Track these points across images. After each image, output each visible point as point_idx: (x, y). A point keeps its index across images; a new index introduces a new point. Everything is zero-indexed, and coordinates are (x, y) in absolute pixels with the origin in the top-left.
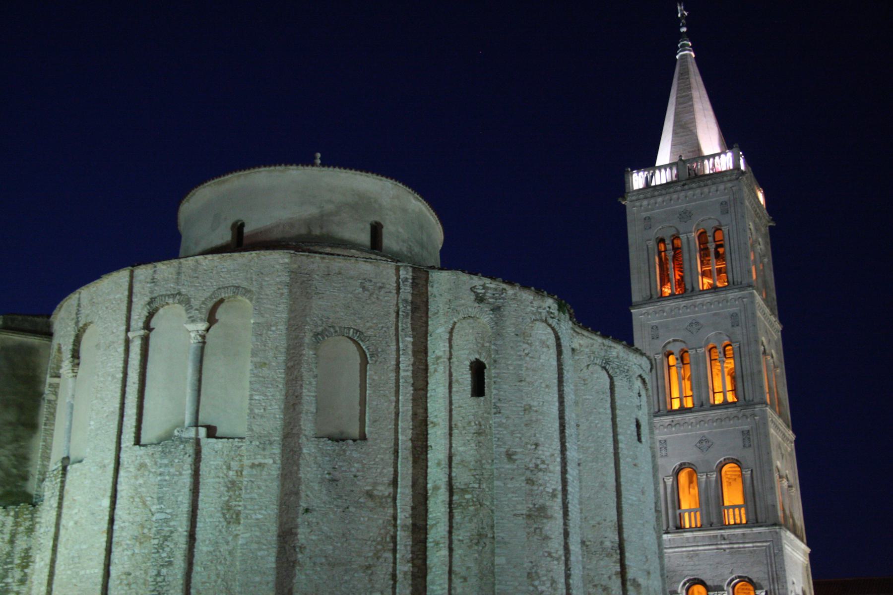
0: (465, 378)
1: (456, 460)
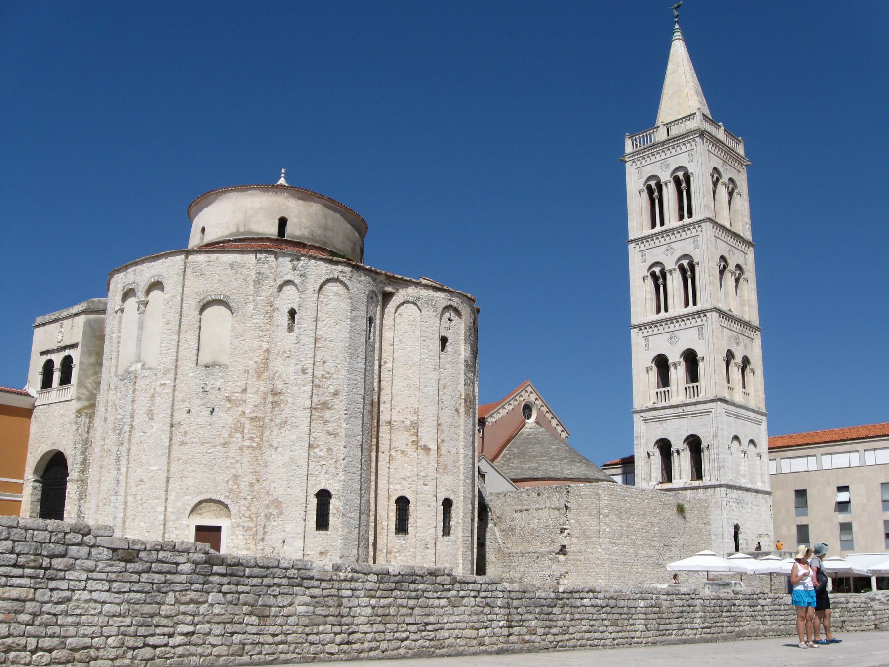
0: (285, 320)
1: (277, 375)
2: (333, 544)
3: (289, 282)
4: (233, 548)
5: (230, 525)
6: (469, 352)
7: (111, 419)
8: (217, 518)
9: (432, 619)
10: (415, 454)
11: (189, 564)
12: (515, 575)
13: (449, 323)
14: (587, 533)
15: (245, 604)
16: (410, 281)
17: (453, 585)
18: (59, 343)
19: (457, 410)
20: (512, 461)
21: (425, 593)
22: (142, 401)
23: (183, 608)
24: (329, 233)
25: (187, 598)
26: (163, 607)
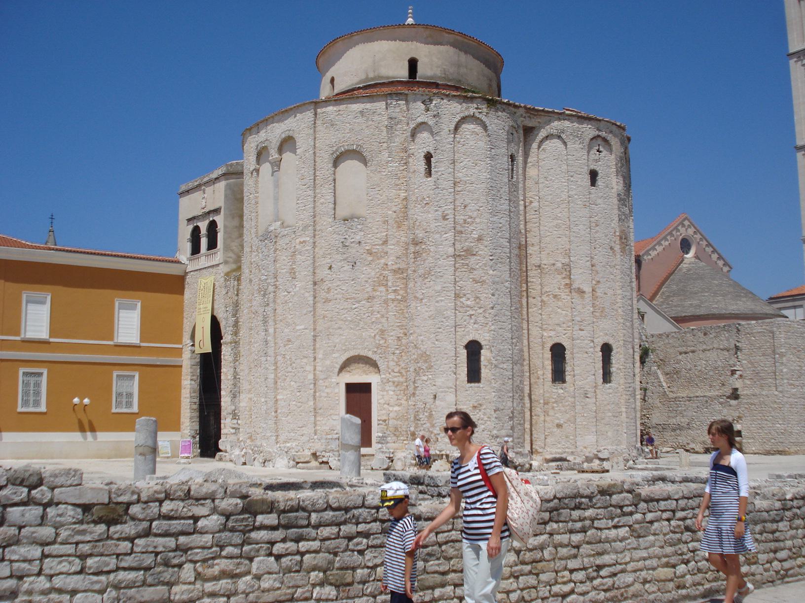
0: (421, 166)
2: (486, 398)
3: (422, 126)
4: (384, 404)
5: (379, 381)
6: (622, 185)
7: (256, 280)
8: (367, 374)
9: (607, 559)
10: (569, 298)
11: (215, 517)
12: (683, 420)
13: (598, 155)
14: (761, 375)
15: (314, 570)
16: (553, 112)
17: (636, 505)
18: (203, 208)
19: (611, 248)
20: (671, 299)
21: (596, 522)
22: (284, 260)
23: (209, 587)
24: (463, 70)
25: (216, 570)
26: (175, 589)
